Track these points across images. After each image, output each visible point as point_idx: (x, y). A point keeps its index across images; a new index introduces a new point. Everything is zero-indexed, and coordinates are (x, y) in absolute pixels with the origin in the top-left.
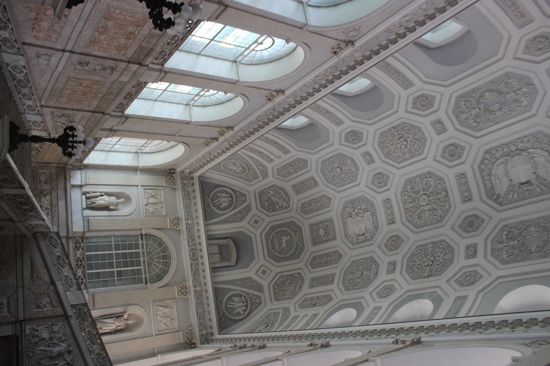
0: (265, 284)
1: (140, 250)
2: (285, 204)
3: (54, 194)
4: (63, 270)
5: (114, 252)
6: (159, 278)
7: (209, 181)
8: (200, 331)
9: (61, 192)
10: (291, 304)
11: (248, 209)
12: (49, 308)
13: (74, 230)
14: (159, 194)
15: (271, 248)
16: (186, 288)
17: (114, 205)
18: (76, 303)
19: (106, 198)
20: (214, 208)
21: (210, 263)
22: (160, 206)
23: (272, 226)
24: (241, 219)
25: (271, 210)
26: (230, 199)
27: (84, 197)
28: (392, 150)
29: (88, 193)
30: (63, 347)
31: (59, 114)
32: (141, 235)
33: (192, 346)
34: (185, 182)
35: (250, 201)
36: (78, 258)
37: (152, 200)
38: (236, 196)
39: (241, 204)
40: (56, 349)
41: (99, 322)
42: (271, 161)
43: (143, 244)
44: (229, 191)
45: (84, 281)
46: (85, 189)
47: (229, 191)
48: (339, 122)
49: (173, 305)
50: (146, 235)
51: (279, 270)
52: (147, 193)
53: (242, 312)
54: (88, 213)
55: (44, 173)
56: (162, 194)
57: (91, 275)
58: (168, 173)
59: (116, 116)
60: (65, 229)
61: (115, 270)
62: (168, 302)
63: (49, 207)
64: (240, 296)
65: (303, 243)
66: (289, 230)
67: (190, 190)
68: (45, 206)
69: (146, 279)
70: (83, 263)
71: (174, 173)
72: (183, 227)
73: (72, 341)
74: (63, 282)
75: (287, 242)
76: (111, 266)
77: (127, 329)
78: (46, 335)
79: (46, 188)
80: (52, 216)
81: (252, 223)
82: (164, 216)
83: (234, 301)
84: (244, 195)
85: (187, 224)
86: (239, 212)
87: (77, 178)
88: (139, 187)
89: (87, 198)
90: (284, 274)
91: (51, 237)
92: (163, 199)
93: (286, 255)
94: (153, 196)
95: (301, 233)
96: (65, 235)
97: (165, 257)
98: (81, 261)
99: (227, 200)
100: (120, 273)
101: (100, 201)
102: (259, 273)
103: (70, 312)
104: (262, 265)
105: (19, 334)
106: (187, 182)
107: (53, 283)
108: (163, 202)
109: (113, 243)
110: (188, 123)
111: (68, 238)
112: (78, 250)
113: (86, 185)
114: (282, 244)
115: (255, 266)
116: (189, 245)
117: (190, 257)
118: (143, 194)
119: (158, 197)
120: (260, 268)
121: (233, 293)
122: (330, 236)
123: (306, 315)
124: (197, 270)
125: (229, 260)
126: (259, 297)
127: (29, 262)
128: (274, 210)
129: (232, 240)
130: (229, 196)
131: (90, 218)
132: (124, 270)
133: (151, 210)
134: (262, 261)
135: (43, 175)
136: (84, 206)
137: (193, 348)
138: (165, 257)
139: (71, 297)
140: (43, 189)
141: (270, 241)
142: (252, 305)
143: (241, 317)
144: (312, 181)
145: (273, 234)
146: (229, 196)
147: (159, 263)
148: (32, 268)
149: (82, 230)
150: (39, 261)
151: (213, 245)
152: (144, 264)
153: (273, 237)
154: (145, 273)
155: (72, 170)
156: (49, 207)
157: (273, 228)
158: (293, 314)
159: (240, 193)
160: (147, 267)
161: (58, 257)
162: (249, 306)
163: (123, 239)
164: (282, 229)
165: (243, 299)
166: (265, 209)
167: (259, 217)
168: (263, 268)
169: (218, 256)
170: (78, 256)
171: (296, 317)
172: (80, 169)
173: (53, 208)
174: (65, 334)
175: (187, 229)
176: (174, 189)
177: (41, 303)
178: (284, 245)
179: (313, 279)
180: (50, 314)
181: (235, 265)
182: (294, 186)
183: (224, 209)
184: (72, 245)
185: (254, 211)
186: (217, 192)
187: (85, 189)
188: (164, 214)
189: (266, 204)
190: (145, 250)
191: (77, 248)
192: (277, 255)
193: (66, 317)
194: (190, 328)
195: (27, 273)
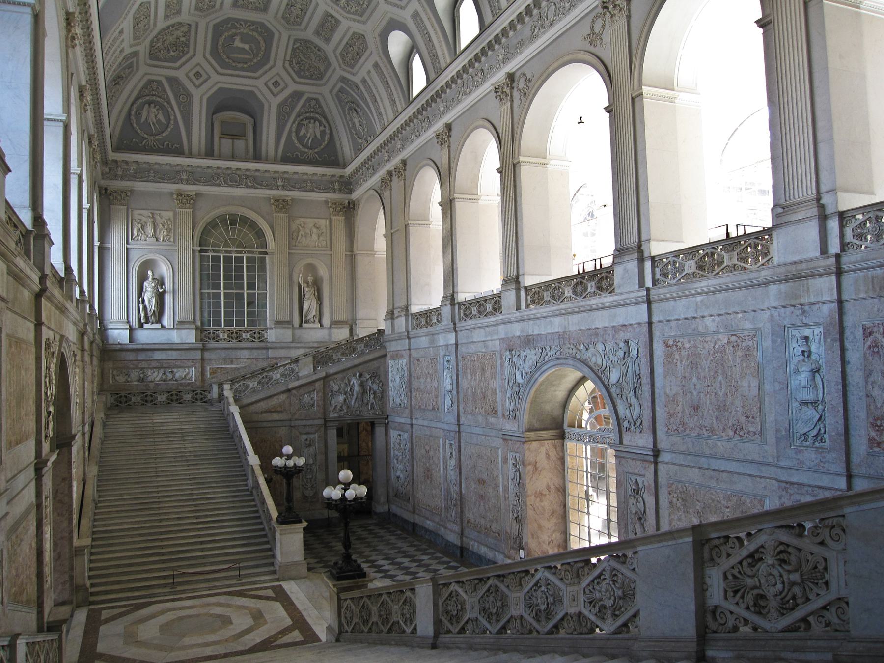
0: (292, 87)
2: (182, 29)
3: (144, 365)
4: (274, 378)
5: (222, 291)
6: (260, 234)
10: (337, 71)
11: (173, 81)
12: (315, 395)
13: (194, 341)
14: (140, 217)
16: (278, 201)
18: (312, 366)
20: (164, 134)
21: (246, 159)
22: (158, 217)
24: (189, 96)
26: (152, 105)
27: (145, 326)
29: (139, 319)
30: (355, 381)
32: (201, 251)
33: (351, 206)
37: (150, 230)
38: (150, 94)
39: (164, 91)
40: (357, 388)
41: (306, 316)
42: (122, 51)
43: (214, 251)
46: (135, 324)
49: (298, 222)
51: (280, 63)
53: (322, 128)
54: (167, 320)
55: (114, 376)
57: (251, 322)
60: (192, 352)
61: (245, 291)
62: (294, 227)
63: (162, 371)
64: (300, 125)
65: (253, 23)
67: (133, 167)
69: (261, 253)
71: (106, 189)
72: (191, 189)
73: (350, 373)
75: (242, 41)
76: (240, 296)
77: (317, 285)
78: (341, 398)
79: (136, 374)
81: (198, 82)
82: (175, 215)
83: (305, 136)
84: (150, 82)
85: (188, 182)
86: (177, 97)
87: (119, 334)
88: (129, 246)
89: (147, 322)
90: (288, 58)
92: (146, 213)
93: (263, 49)
94: (143, 227)
97: (233, 223)
99: (154, 110)
100: (251, 286)
102: (276, 91)
103: (323, 374)
104: (266, 84)
105: (336, 424)
107: (289, 391)
108: (153, 214)
109: (211, 291)
111: (204, 349)
112: (218, 336)
113: (128, 322)
116: (219, 185)
117: (237, 186)
119: (144, 219)
120: (269, 89)
121: (294, 134)
123: (369, 72)
125: (244, 125)
126: (309, 100)
127: (265, 415)
129: (213, 114)
131: (177, 319)
134: (260, 83)
135: (117, 378)
136: (159, 326)
137: (354, 205)
139: (306, 370)
140: (137, 378)
142: (314, 111)
143: (328, 131)
148: (270, 412)
150: (263, 405)
151: (220, 146)
152: (240, 252)
153: (228, 58)
154: (252, 252)
156: (162, 371)
157: (215, 53)
158: (357, 79)
160: (245, 250)
161: (259, 383)
162: (317, 116)
163: (205, 277)
164: (220, 43)
165: (305, 122)
166: (181, 57)
167: (191, 70)
168: (270, 84)
171: (364, 81)
172: (106, 329)
174: (343, 379)
175: (195, 184)
176: (132, 191)
178: (247, 47)
179: (317, 33)
180: (321, 394)
182: (166, 17)
184: (212, 344)
185: (180, 74)
188: (170, 214)
189: (172, 53)
190: (222, 249)
191: (216, 339)
192: (258, 61)
193: (327, 376)
195: (276, 416)
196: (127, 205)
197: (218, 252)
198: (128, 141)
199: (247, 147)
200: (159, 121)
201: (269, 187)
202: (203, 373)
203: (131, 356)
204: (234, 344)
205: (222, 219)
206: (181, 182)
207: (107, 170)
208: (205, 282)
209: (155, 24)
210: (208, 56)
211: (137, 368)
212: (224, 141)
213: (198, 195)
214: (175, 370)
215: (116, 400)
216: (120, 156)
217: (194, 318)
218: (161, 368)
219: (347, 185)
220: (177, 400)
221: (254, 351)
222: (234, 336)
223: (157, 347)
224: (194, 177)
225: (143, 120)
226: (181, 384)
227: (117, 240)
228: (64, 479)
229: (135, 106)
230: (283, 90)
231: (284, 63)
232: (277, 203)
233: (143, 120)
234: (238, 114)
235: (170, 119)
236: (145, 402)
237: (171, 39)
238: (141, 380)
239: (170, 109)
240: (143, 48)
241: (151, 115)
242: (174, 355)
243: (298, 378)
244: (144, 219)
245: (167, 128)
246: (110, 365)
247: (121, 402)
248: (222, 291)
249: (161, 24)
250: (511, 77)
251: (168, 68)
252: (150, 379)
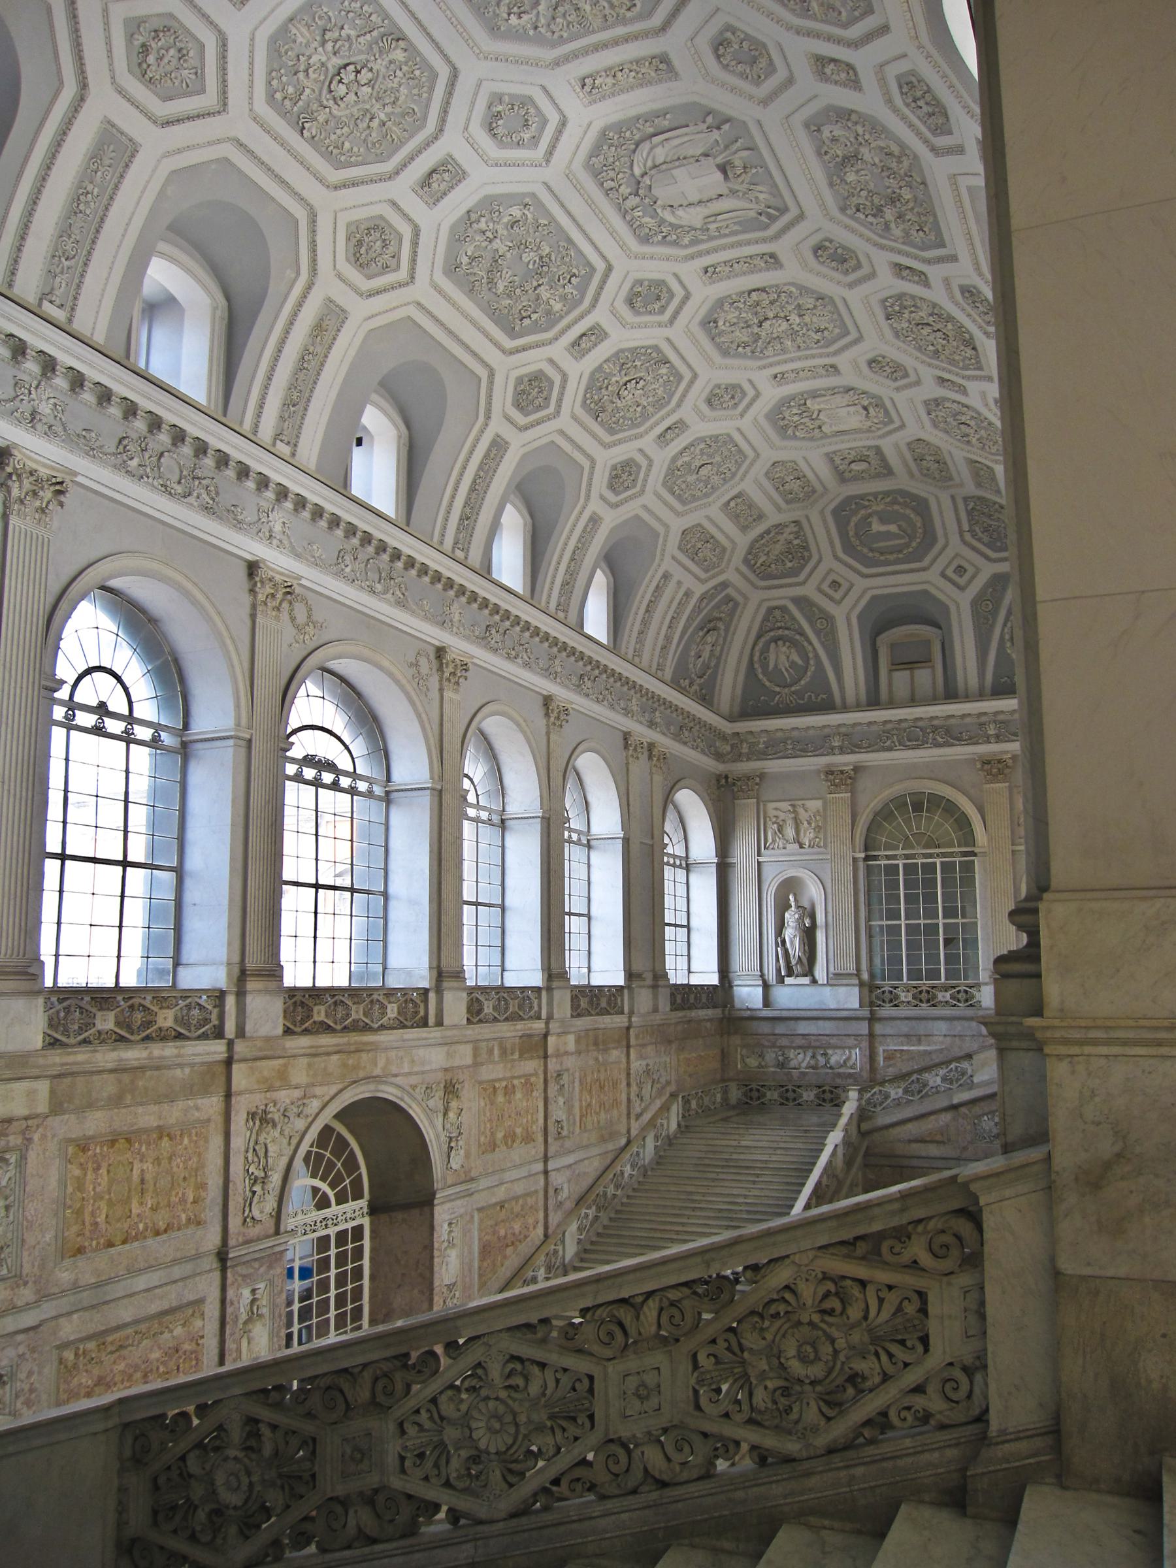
1: (901, 863)
3: (784, 1042)
4: (931, 1083)
5: (903, 922)
6: (963, 823)
7: (739, 691)
9: (780, 1029)
13: (857, 1006)
15: (901, 556)
16: (988, 762)
17: (800, 920)
19: (789, 933)
20: (803, 682)
21: (934, 700)
22: (801, 811)
23: (845, 552)
24: (829, 619)
25: (806, 554)
27: (788, 980)
28: (650, 399)
29: (778, 970)
31: (638, 1102)
34: (745, 750)
36: (914, 997)
37: (790, 832)
38: (776, 628)
39: (794, 619)
42: (688, 594)
43: (888, 857)
44: (760, 645)
45: (962, 988)
46: (772, 977)
47: (760, 645)
48: (595, 520)
50: (866, 849)
51: (955, 539)
52: (774, 841)
54: (820, 972)
56: (777, 809)
58: (727, 801)
59: (631, 998)
61: (941, 921)
63: (809, 1054)
65: (887, 494)
66: (854, 519)
68: (808, 1059)
69: (965, 854)
70: (924, 988)
71: (726, 777)
72: (846, 760)
74: (955, 1086)
75: (883, 521)
76: (932, 930)
80: (829, 1048)
81: (837, 596)
84: (771, 610)
85: (842, 751)
86: (812, 624)
88: (761, 859)
89: (790, 973)
90: (966, 527)
91: (868, 1102)
92: (785, 806)
95: (862, 497)
96: (865, 1024)
97: (918, 807)
98: (921, 992)
99: (784, 649)
100: (949, 912)
101: (795, 947)
102: (961, 581)
104: (943, 575)
106: (745, 745)
107: (955, 1107)
108: (793, 806)
109: (885, 923)
110: (626, 841)
111: (872, 1019)
112: (897, 997)
113: (762, 976)
114: (888, 532)
115: (944, 591)
116: (890, 749)
118: (777, 852)
119: (782, 816)
124: (948, 731)
127: (914, 1145)
128: (806, 548)
129: (878, 633)
130: (773, 645)
131: (831, 969)
132: (943, 902)
133: (812, 835)
134: (933, 575)
135: (748, 1060)
136: (806, 980)
138: (918, 807)
141: (882, 558)
144: (732, 504)
145: (865, 550)
146: (773, 645)
147: (929, 819)
149: (857, 989)
150: (913, 1129)
151: (890, 685)
152: (930, 856)
153: (872, 550)
154: (951, 855)
155: (733, 1006)
157: (849, 548)
159: (766, 619)
160: (938, 851)
161: (906, 1091)
164: (851, 533)
166: (803, 567)
168: (950, 572)
169: (917, 673)
170: (910, 999)
172: (731, 987)
173: (813, 1044)
175: (853, 752)
176: (762, 776)
177: (990, 1131)
178: (893, 528)
181: (940, 628)
183: (806, 659)
184: (886, 1011)
186: (764, 674)
187: (772, 977)
188: (818, 804)
189: (789, 565)
190: (900, 852)
191: (894, 1001)
192: (920, 541)
196: (758, 798)
197: (894, 857)
198: (754, 705)
199: (934, 679)
200: (793, 664)
201: (972, 741)
202: (872, 1057)
203: (765, 1028)
204: (925, 1010)
205: (899, 803)
206: (831, 751)
207: (728, 748)
208: (875, 907)
210: (841, 554)
211: (773, 1046)
212: (897, 675)
213: (857, 769)
214: (830, 1052)
215: (745, 1094)
216: (742, 727)
217: (858, 969)
218: (809, 1047)
220: (832, 1100)
221: (955, 1022)
222: (924, 996)
223: (803, 1014)
224: (852, 742)
225: (771, 666)
226: (839, 1075)
227: (743, 852)
228: (425, 1247)
229: (757, 648)
230: (973, 577)
231: (961, 536)
232: (986, 767)
233: (771, 666)
234: (917, 626)
235: (808, 658)
236: (785, 1100)
237: (778, 548)
238: (782, 1065)
239: (806, 644)
241: (782, 657)
242: (827, 1027)
243: (971, 1086)
244: (782, 816)
246: (736, 1040)
247: (751, 1099)
249: (743, 541)
252: (793, 1063)
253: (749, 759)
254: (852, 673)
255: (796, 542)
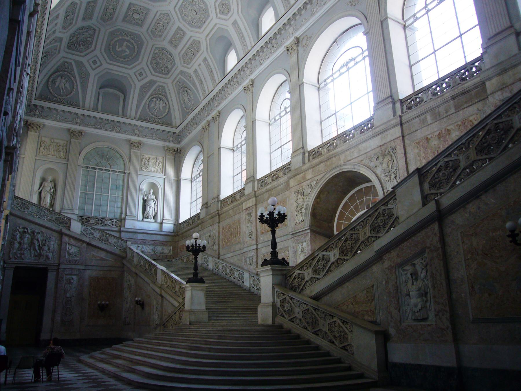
0: (150, 77)
2: (90, 32)
8: (170, 142)
11: (80, 64)
23: (105, 51)
24: (88, 75)
33: (179, 151)
35: (74, 60)
38: (63, 71)
53: (164, 105)
83: (154, 107)
98: (98, 220)
99: (64, 81)
104: (135, 73)
116: (100, 129)
122: (145, 12)
126: (159, 86)
129: (100, 88)
130: (60, 78)
134: (131, 72)
141: (117, 58)
143: (168, 107)
146: (60, 78)
158: (191, 71)
165: (154, 100)
168: (137, 74)
171: (196, 71)
176: (44, 125)
179: (171, 42)
182: (84, 19)
185: (84, 60)
194: (166, 149)
209: (76, 23)
216: (39, 103)
219: (178, 137)
225: (57, 85)
229: (53, 76)
230: (144, 78)
233: (57, 85)
240: (66, 37)
245: (71, 93)
248: (95, 193)
249: (80, 24)
250: (298, 40)
251: (78, 55)
253: (38, 117)
254: (90, 99)
255: (88, 39)
